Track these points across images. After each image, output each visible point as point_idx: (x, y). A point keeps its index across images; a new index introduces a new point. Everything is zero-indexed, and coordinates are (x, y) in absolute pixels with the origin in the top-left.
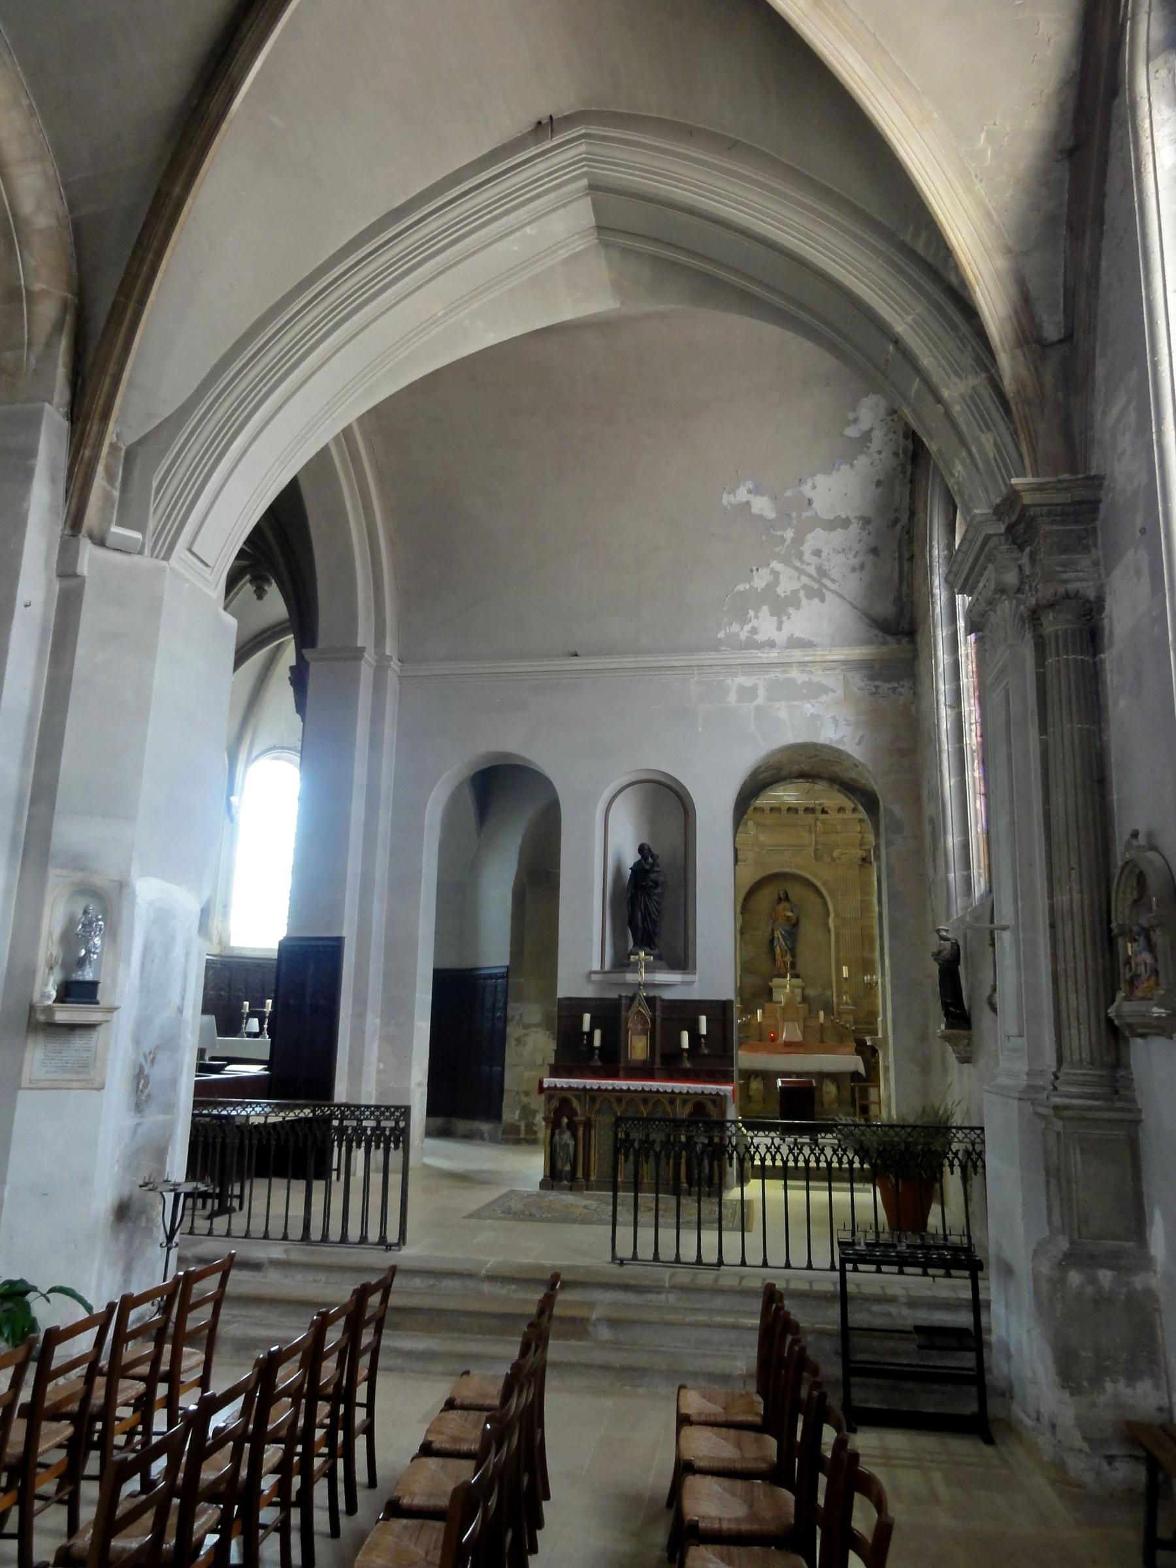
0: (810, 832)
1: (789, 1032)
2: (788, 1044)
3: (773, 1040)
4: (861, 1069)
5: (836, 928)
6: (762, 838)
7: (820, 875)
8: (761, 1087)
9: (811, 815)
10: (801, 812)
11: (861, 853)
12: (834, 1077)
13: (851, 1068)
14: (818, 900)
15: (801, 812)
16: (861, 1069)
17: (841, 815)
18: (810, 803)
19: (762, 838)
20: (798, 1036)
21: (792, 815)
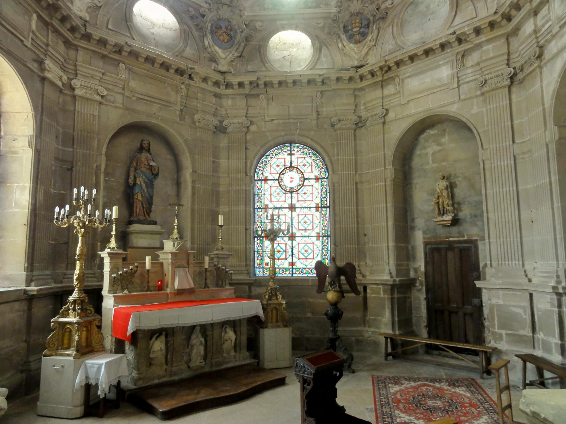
0: (177, 93)
1: (178, 281)
2: (180, 292)
3: (160, 288)
4: (261, 313)
5: (193, 182)
6: (133, 84)
7: (180, 135)
8: (163, 347)
9: (179, 77)
10: (172, 71)
11: (215, 121)
12: (233, 324)
13: (252, 313)
14: (169, 157)
15: (172, 71)
16: (261, 313)
17: (203, 85)
18: (183, 65)
19: (133, 84)
20: (189, 283)
21: (163, 72)
